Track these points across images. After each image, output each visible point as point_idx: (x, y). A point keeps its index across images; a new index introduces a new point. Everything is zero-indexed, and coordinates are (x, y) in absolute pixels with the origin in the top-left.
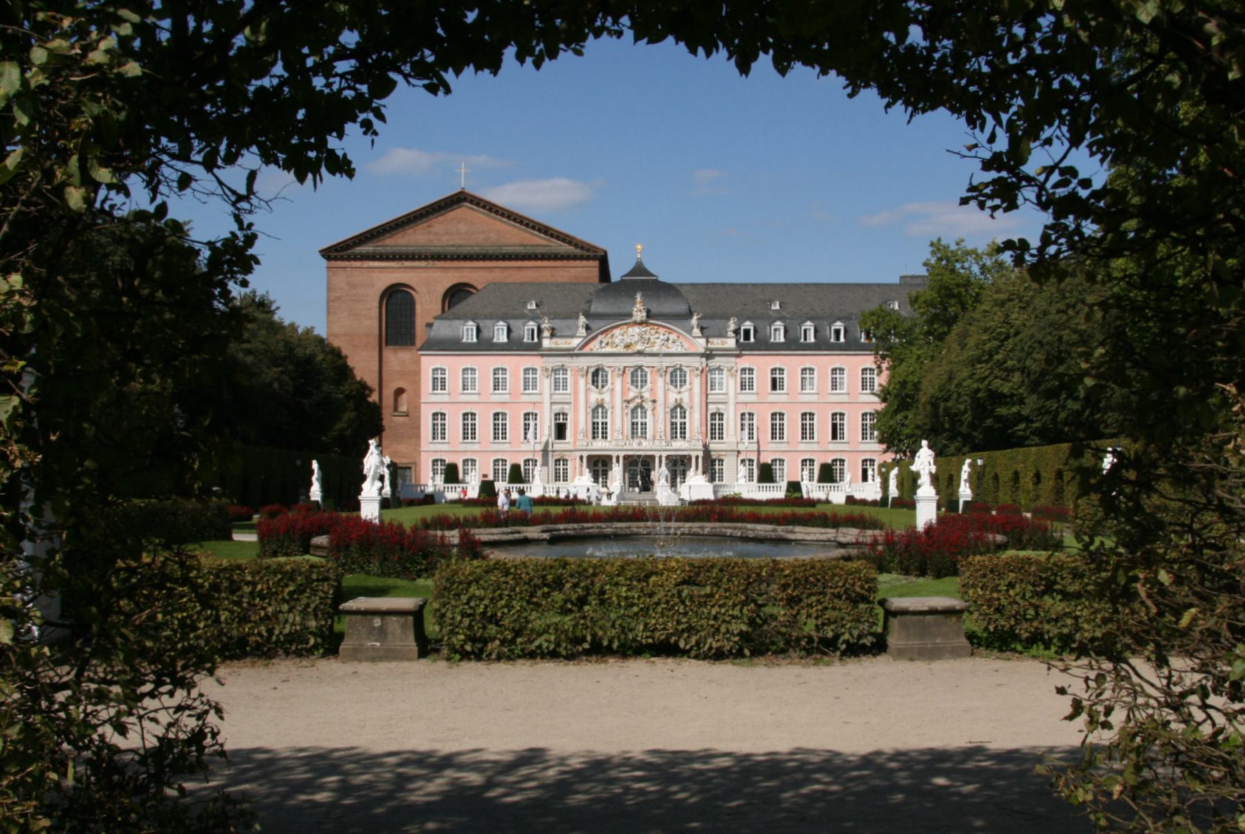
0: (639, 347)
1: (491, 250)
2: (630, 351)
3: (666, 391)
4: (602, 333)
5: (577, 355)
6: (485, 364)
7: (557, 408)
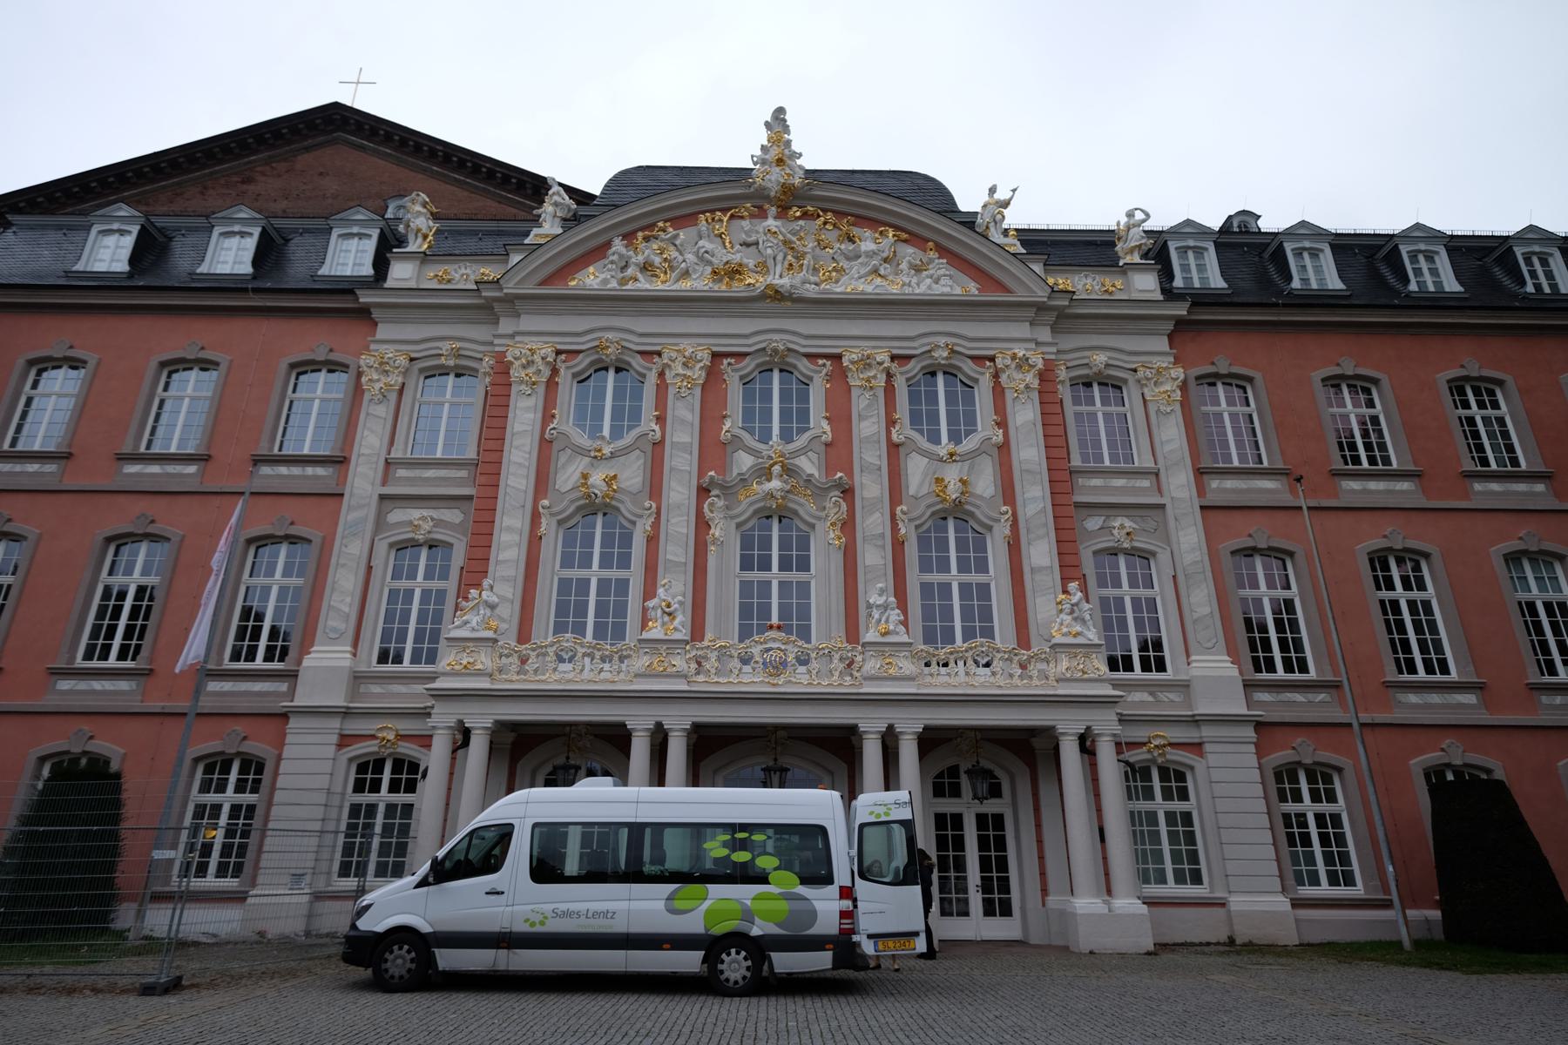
2: (737, 288)
3: (894, 448)
5: (514, 305)
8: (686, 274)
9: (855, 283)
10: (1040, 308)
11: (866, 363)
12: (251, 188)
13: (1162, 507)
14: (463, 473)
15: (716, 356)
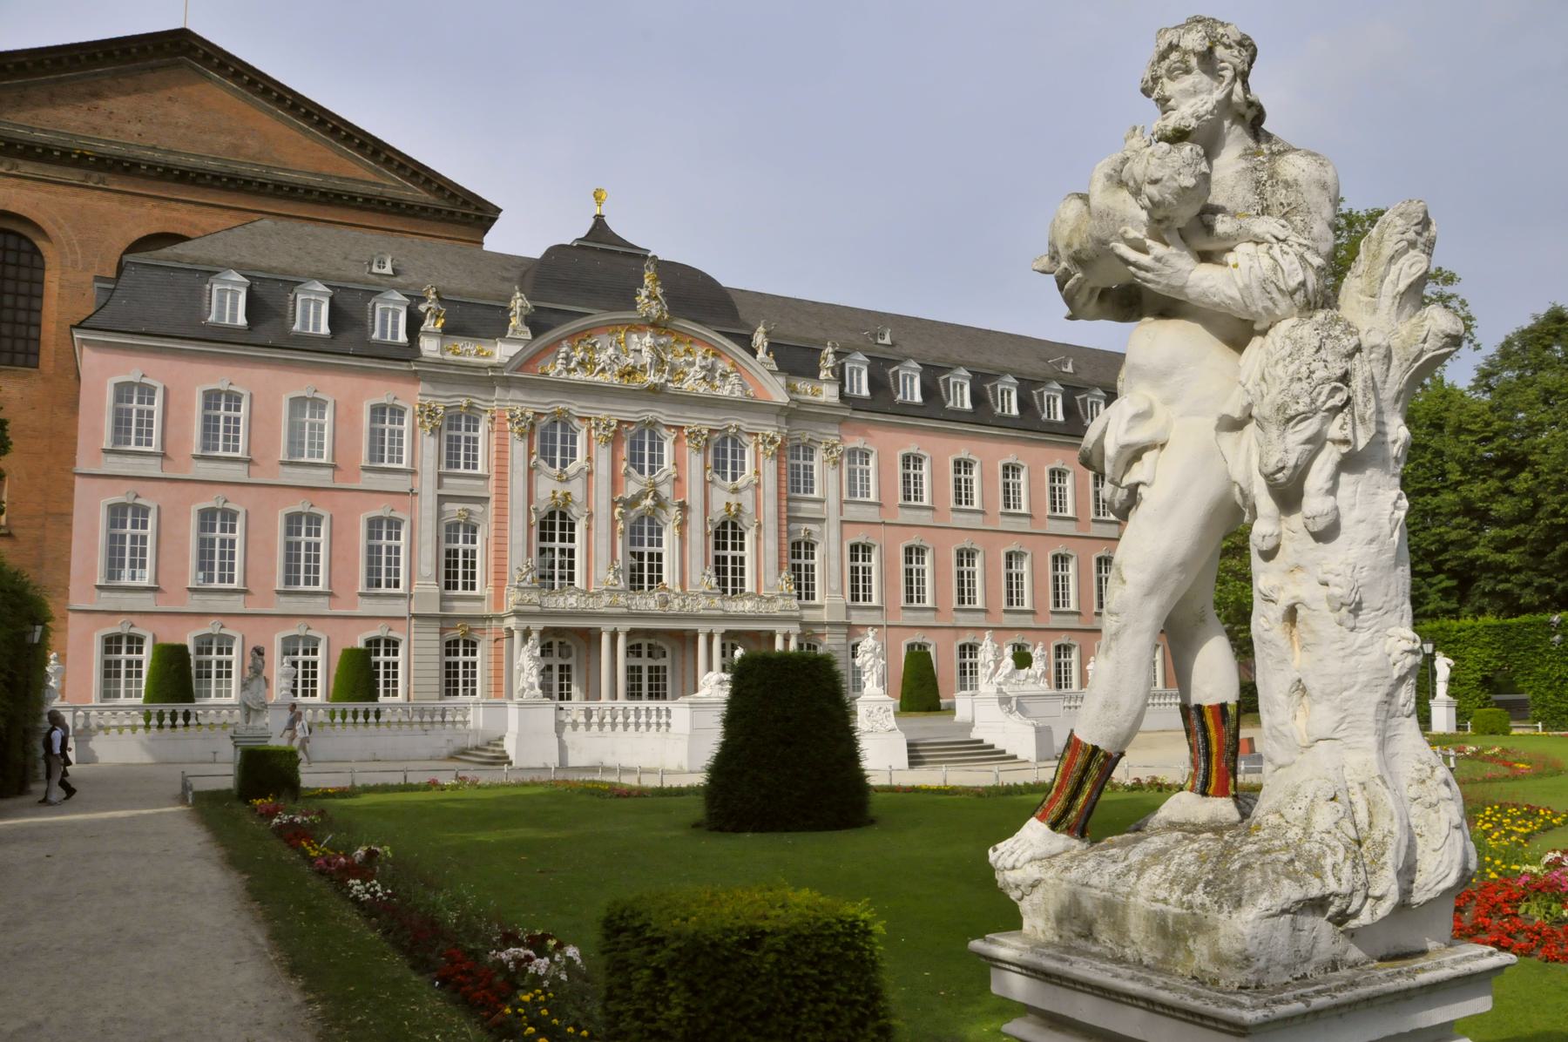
0: (652, 378)
1: (247, 171)
2: (635, 385)
4: (571, 337)
5: (508, 383)
6: (269, 388)
7: (454, 510)
8: (603, 370)
9: (692, 383)
10: (783, 408)
11: (694, 435)
12: (102, 103)
13: (822, 520)
14: (480, 483)
15: (620, 422)
